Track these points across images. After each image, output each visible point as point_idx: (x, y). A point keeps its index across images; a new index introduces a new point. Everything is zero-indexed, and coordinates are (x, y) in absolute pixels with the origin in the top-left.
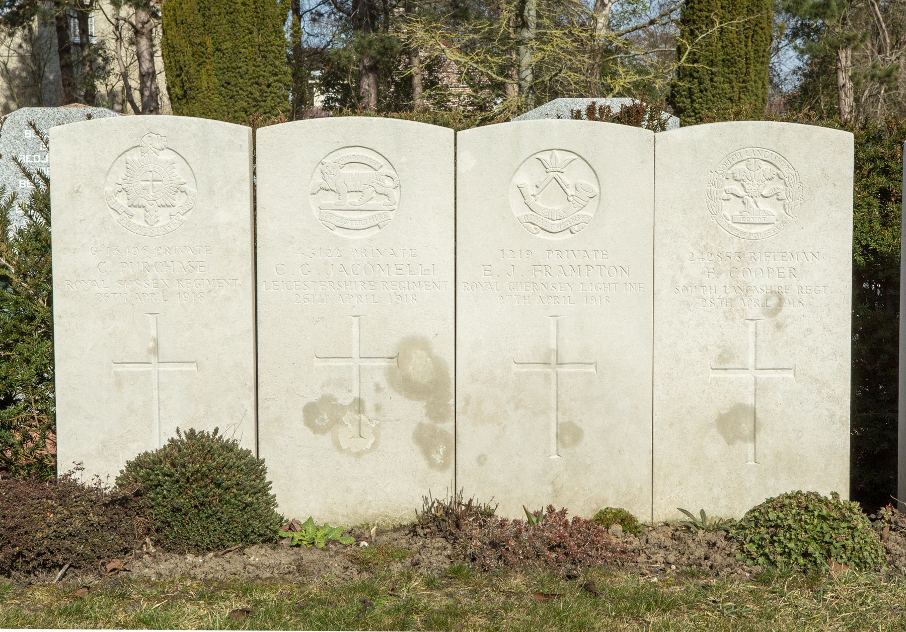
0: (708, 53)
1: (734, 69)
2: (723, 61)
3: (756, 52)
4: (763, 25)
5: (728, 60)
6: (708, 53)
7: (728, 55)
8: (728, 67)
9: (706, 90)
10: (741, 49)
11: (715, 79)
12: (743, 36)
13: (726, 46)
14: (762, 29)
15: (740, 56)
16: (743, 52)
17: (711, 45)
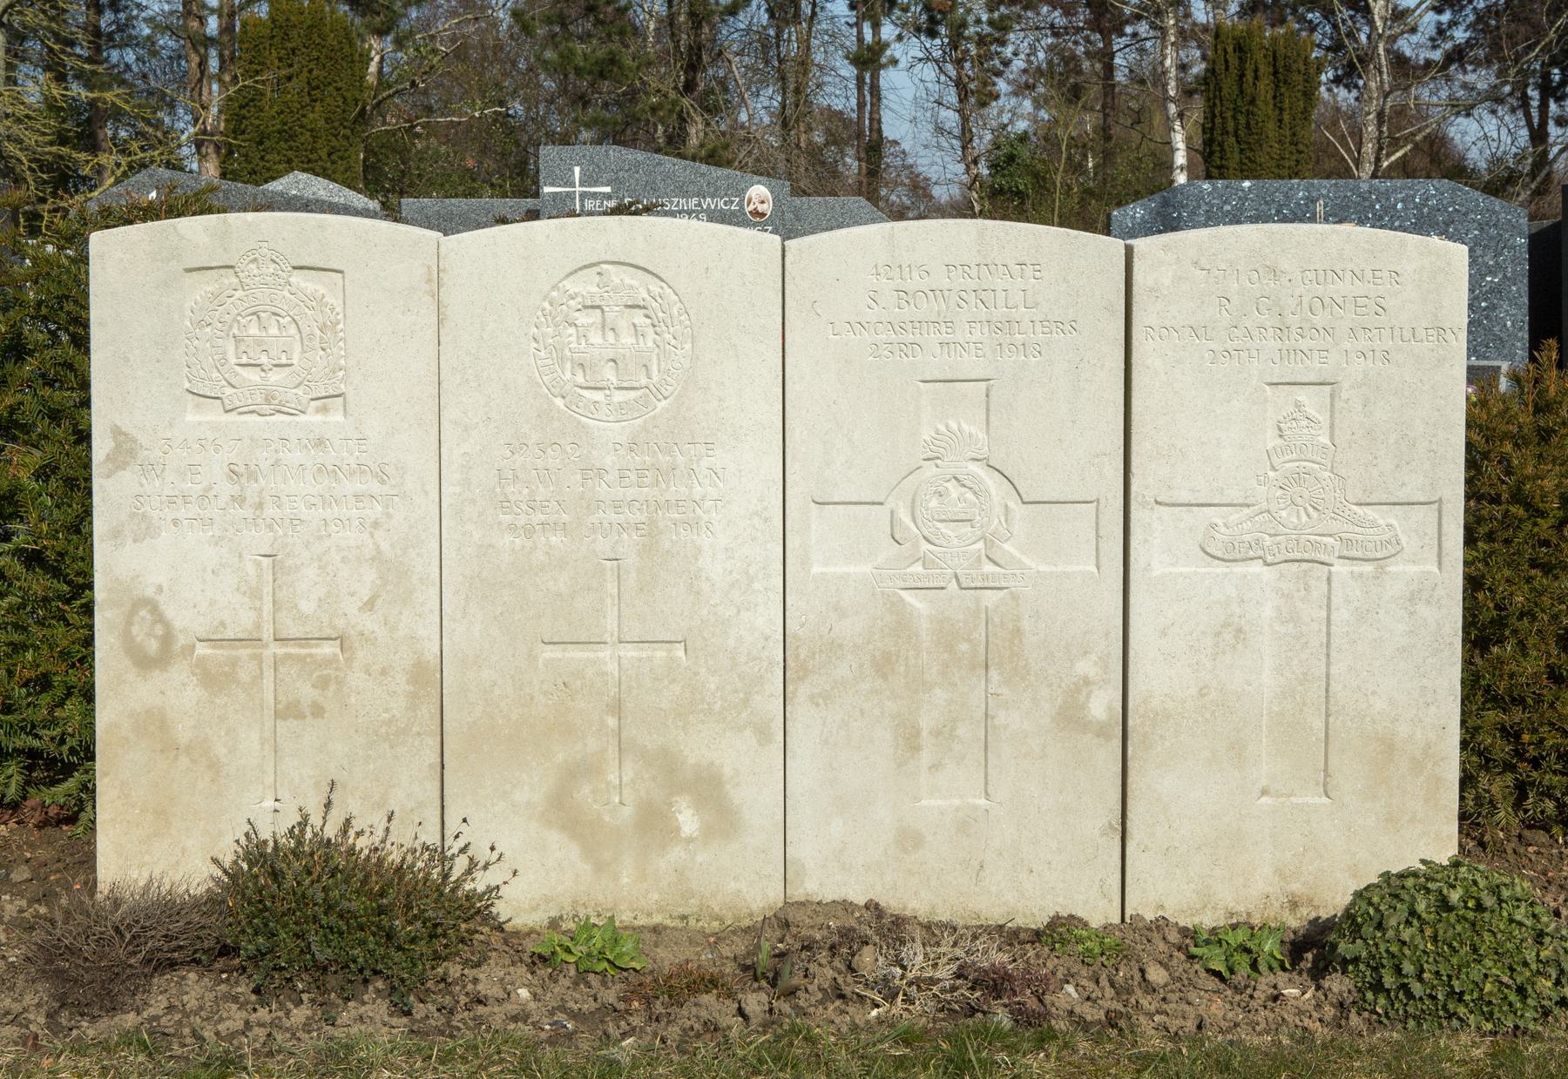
0: (257, 122)
1: (293, 144)
2: (279, 132)
3: (327, 120)
4: (339, 85)
5: (285, 131)
6: (257, 122)
7: (285, 124)
8: (286, 141)
9: (255, 173)
10: (304, 116)
11: (268, 157)
12: (307, 99)
13: (282, 112)
14: (338, 89)
15: (301, 126)
16: (305, 121)
17: (261, 111)
